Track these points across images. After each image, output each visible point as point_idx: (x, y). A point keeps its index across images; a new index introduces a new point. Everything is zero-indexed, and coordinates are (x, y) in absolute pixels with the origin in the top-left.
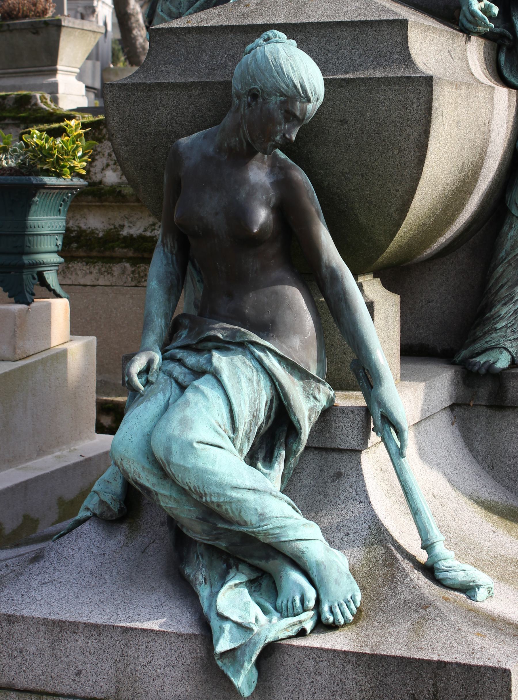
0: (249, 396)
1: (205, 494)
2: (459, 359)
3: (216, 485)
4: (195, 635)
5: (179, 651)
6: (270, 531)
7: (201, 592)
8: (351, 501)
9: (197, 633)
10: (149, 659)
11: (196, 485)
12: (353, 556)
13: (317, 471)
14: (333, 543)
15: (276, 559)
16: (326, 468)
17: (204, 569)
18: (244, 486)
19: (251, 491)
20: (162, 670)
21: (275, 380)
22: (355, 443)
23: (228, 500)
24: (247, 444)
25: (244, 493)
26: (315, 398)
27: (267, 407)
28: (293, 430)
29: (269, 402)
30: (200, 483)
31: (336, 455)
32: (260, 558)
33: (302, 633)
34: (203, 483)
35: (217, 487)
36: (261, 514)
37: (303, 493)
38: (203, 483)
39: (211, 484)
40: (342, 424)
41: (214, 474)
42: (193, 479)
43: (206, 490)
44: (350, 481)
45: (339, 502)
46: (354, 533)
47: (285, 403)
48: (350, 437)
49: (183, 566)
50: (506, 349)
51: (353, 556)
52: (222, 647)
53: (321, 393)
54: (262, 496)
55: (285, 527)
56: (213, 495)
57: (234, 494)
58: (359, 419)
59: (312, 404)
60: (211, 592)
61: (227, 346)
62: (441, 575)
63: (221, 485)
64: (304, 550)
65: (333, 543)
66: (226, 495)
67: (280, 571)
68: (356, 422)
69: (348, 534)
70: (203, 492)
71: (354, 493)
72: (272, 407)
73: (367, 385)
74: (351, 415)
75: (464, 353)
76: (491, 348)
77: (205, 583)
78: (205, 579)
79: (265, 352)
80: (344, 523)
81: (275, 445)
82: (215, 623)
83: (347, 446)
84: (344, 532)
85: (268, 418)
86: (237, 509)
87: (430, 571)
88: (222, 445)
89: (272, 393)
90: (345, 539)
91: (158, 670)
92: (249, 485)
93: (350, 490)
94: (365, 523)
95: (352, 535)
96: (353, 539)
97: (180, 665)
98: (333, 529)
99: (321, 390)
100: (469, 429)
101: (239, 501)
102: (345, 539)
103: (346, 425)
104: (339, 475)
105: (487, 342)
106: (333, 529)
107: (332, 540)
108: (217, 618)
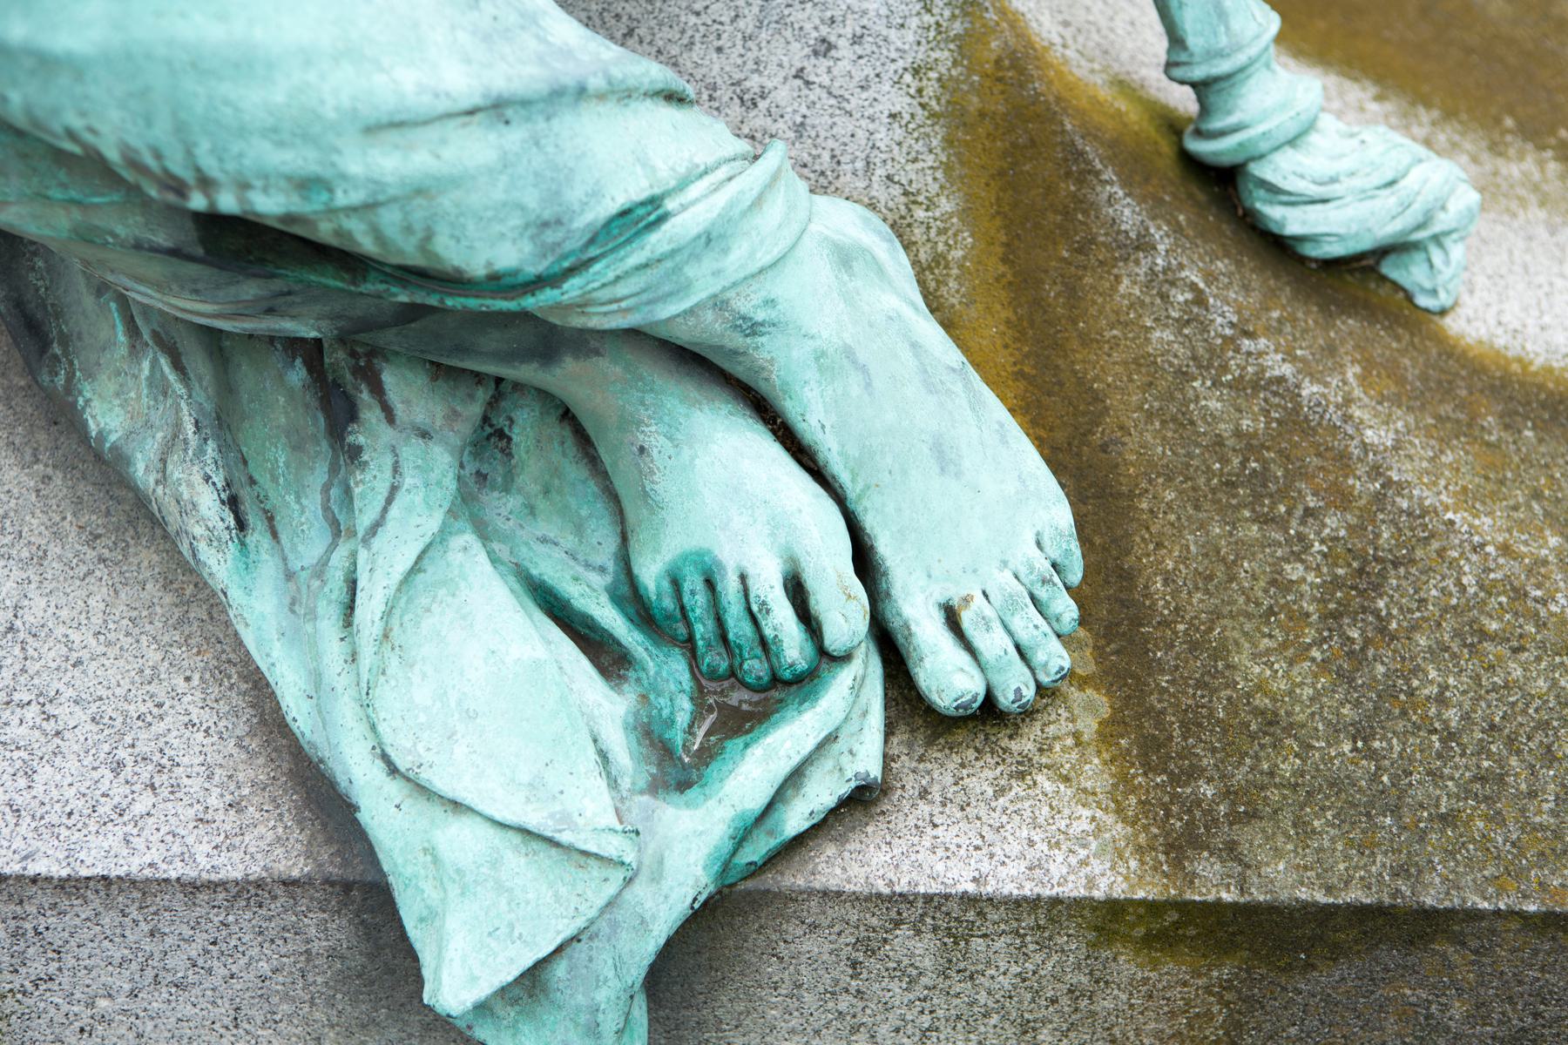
1: (206, 183)
3: (273, 133)
4: (290, 883)
5: (201, 939)
7: (236, 595)
9: (298, 868)
10: (37, 967)
11: (135, 142)
12: (880, 172)
14: (763, 105)
15: (597, 353)
17: (211, 448)
18: (443, 106)
19: (479, 117)
20: (121, 999)
23: (356, 197)
25: (444, 141)
30: (161, 133)
32: (510, 357)
33: (861, 801)
34: (180, 128)
35: (281, 144)
36: (545, 225)
38: (180, 128)
39: (242, 132)
41: (247, 64)
42: (115, 115)
43: (210, 165)
46: (857, 40)
49: (61, 380)
51: (880, 172)
52: (474, 979)
54: (541, 125)
55: (673, 253)
56: (258, 183)
57: (389, 163)
60: (290, 576)
62: (1292, 221)
64: (760, 316)
65: (763, 105)
66: (344, 177)
67: (629, 423)
69: (825, 48)
70: (187, 175)
77: (241, 525)
78: (233, 503)
82: (383, 813)
86: (408, 230)
87: (1220, 188)
90: (818, 71)
91: (103, 1003)
92: (462, 82)
95: (844, 50)
96: (858, 76)
97: (216, 981)
102: (818, 71)
107: (754, 83)
108: (394, 788)
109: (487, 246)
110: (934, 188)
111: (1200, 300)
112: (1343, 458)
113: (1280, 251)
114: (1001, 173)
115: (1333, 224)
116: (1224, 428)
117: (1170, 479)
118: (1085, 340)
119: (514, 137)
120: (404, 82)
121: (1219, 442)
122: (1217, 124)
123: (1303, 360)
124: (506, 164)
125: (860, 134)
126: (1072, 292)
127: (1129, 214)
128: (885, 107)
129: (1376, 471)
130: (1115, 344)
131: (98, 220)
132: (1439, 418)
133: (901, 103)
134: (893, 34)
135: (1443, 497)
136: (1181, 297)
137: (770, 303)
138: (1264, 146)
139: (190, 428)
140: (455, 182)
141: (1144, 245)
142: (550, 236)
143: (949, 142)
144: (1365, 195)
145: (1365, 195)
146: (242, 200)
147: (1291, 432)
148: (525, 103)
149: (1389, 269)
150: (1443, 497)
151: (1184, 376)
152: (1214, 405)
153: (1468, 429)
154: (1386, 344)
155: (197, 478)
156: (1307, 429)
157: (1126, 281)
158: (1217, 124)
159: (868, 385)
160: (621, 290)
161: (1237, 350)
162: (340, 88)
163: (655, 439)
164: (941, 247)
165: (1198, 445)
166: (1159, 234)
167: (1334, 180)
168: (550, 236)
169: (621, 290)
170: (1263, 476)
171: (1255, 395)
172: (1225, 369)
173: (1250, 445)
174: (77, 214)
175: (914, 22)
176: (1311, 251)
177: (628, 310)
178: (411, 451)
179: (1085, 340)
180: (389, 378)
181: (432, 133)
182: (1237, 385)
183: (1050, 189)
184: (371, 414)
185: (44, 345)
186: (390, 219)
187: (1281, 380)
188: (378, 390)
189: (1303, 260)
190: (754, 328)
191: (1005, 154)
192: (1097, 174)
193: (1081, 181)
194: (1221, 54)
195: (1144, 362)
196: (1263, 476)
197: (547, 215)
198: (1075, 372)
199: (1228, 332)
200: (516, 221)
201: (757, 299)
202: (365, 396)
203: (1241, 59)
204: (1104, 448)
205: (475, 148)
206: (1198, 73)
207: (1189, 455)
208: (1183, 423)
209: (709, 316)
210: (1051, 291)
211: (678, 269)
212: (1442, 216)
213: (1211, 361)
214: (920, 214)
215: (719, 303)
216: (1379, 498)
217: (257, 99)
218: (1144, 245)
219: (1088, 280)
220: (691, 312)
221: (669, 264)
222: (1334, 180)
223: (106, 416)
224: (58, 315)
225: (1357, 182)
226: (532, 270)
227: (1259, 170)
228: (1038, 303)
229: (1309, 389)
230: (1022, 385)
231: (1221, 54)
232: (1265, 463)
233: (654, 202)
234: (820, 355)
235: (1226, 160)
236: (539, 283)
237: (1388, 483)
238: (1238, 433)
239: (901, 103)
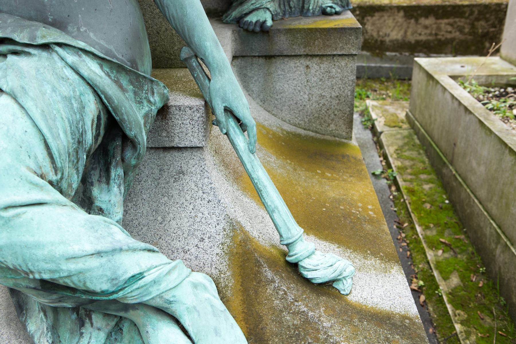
0: (69, 120)
1: (32, 272)
2: (231, 19)
3: (44, 260)
6: (127, 295)
8: (199, 201)
11: (15, 264)
12: (214, 266)
13: (157, 171)
14: (188, 253)
15: (137, 309)
16: (166, 167)
19: (94, 256)
21: (100, 93)
22: (195, 140)
23: (65, 274)
24: (76, 176)
25: (86, 261)
26: (149, 102)
27: (95, 126)
28: (128, 141)
29: (96, 120)
30: (20, 261)
31: (176, 154)
34: (24, 260)
35: (47, 263)
36: (113, 279)
37: (144, 196)
38: (24, 260)
39: (38, 260)
40: (180, 122)
41: (38, 246)
42: (10, 258)
43: (31, 268)
44: (195, 179)
45: (185, 204)
46: (209, 238)
47: (117, 118)
48: (189, 135)
49: (24, 319)
50: (268, 9)
51: (214, 266)
53: (155, 95)
54: (111, 257)
55: (145, 285)
56: (43, 272)
57: (72, 267)
58: (198, 115)
59: (147, 109)
61: (27, 50)
62: (309, 275)
63: (51, 259)
64: (172, 299)
65: (188, 253)
66: (62, 270)
67: (145, 326)
68: (196, 118)
69: (202, 240)
70: (28, 271)
71: (201, 192)
72: (100, 124)
73: (203, 76)
74: (189, 112)
75: (235, 13)
76: (257, 9)
79: (80, 56)
80: (196, 227)
81: (110, 163)
83: (188, 144)
84: (197, 237)
85: (96, 137)
86: (80, 281)
88: (42, 201)
89: (98, 108)
90: (201, 245)
92: (90, 248)
93: (196, 189)
94: (218, 224)
95: (207, 240)
96: (209, 245)
98: (185, 235)
99: (155, 91)
100: (245, 75)
101: (80, 272)
102: (201, 245)
103: (184, 122)
104: (182, 172)
105: (252, 4)
106: (185, 235)
107: (187, 248)
109: (100, 285)
110: (226, 270)
111: (286, 293)
112: (318, 330)
113: (308, 281)
114: (241, 266)
115: (319, 275)
116: (290, 324)
117: (277, 336)
118: (259, 304)
119: (104, 260)
120: (76, 249)
121: (289, 327)
122: (291, 254)
123: (310, 307)
124: (101, 266)
125: (210, 258)
126: (256, 292)
127: (269, 274)
128: (215, 252)
129: (325, 333)
130: (266, 304)
131: (18, 282)
132: (343, 320)
133: (219, 251)
134: (217, 236)
135: (341, 339)
136: (281, 293)
137: (174, 296)
138: (301, 258)
139: (45, 329)
140: (89, 270)
141: (273, 281)
142: (115, 282)
143: (229, 259)
144: (325, 269)
145: (325, 269)
146: (40, 276)
147: (306, 324)
148: (106, 252)
149: (335, 285)
150: (341, 339)
151: (281, 311)
152: (288, 318)
153: (350, 322)
154: (332, 302)
155: (45, 341)
156: (310, 323)
157: (269, 289)
158: (291, 254)
159: (199, 315)
160: (133, 294)
161: (294, 305)
162: (60, 250)
163: (150, 329)
164: (227, 283)
165: (284, 328)
166: (277, 279)
167: (318, 265)
168: (115, 282)
169: (133, 294)
170: (299, 335)
171: (298, 315)
172: (291, 309)
173: (296, 327)
174: (14, 281)
175: (222, 234)
176: (314, 281)
177: (136, 299)
178: (95, 333)
179: (259, 304)
180: (93, 316)
181: (83, 259)
182: (294, 313)
183: (252, 269)
184: (88, 325)
185: (22, 311)
186: (75, 279)
187: (304, 312)
188: (91, 319)
189: (313, 284)
190: (170, 302)
191: (242, 262)
192: (263, 265)
193: (259, 267)
194: (290, 238)
195: (273, 308)
196: (299, 335)
197: (113, 277)
198: (256, 311)
199: (292, 301)
200: (105, 279)
201: (170, 295)
202: (87, 321)
203: (294, 239)
204: (262, 329)
205: (94, 263)
206: (285, 242)
207: (281, 330)
208: (281, 322)
209: (158, 300)
210: (251, 292)
211: (147, 289)
212: (344, 273)
213: (287, 308)
214: (222, 276)
215: (160, 296)
216: (326, 339)
217: (40, 253)
218: (273, 281)
219: (260, 290)
220: (153, 298)
221: (145, 288)
222: (318, 265)
223: (31, 327)
224: (26, 304)
225: (323, 266)
226: (113, 289)
227: (300, 263)
228: (248, 295)
229: (310, 314)
230: (244, 314)
231: (290, 238)
232: (299, 331)
233: (141, 274)
234: (187, 308)
235: (294, 262)
236: (113, 293)
237: (328, 336)
238: (293, 325)
239: (219, 251)
